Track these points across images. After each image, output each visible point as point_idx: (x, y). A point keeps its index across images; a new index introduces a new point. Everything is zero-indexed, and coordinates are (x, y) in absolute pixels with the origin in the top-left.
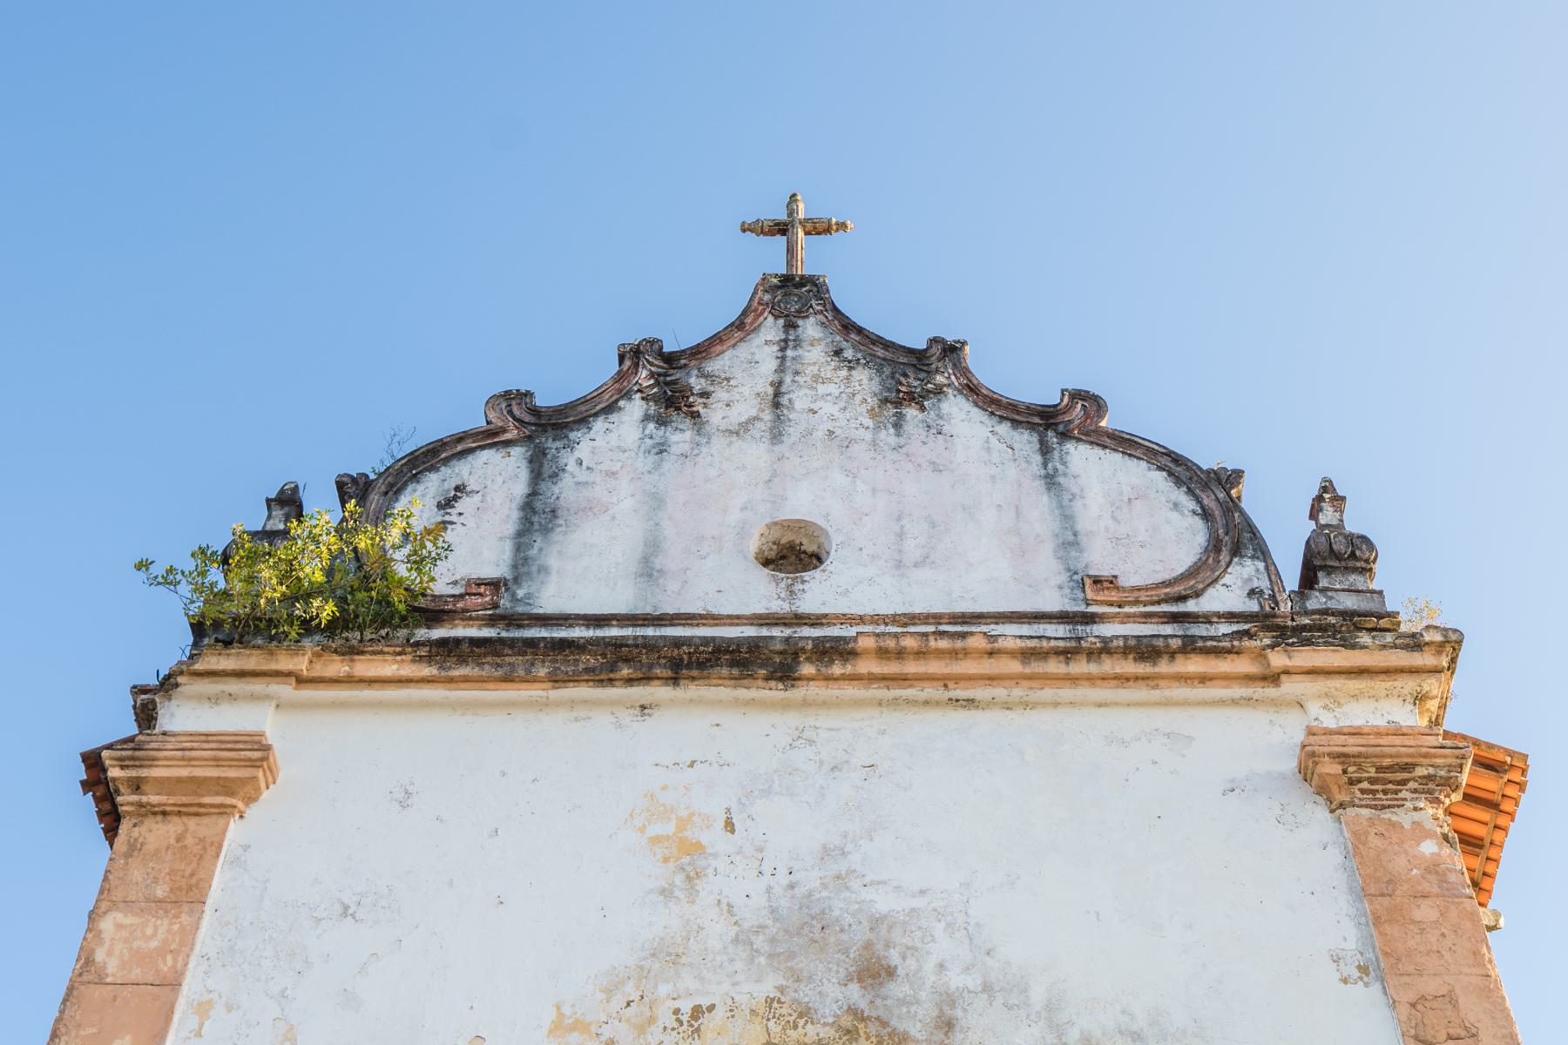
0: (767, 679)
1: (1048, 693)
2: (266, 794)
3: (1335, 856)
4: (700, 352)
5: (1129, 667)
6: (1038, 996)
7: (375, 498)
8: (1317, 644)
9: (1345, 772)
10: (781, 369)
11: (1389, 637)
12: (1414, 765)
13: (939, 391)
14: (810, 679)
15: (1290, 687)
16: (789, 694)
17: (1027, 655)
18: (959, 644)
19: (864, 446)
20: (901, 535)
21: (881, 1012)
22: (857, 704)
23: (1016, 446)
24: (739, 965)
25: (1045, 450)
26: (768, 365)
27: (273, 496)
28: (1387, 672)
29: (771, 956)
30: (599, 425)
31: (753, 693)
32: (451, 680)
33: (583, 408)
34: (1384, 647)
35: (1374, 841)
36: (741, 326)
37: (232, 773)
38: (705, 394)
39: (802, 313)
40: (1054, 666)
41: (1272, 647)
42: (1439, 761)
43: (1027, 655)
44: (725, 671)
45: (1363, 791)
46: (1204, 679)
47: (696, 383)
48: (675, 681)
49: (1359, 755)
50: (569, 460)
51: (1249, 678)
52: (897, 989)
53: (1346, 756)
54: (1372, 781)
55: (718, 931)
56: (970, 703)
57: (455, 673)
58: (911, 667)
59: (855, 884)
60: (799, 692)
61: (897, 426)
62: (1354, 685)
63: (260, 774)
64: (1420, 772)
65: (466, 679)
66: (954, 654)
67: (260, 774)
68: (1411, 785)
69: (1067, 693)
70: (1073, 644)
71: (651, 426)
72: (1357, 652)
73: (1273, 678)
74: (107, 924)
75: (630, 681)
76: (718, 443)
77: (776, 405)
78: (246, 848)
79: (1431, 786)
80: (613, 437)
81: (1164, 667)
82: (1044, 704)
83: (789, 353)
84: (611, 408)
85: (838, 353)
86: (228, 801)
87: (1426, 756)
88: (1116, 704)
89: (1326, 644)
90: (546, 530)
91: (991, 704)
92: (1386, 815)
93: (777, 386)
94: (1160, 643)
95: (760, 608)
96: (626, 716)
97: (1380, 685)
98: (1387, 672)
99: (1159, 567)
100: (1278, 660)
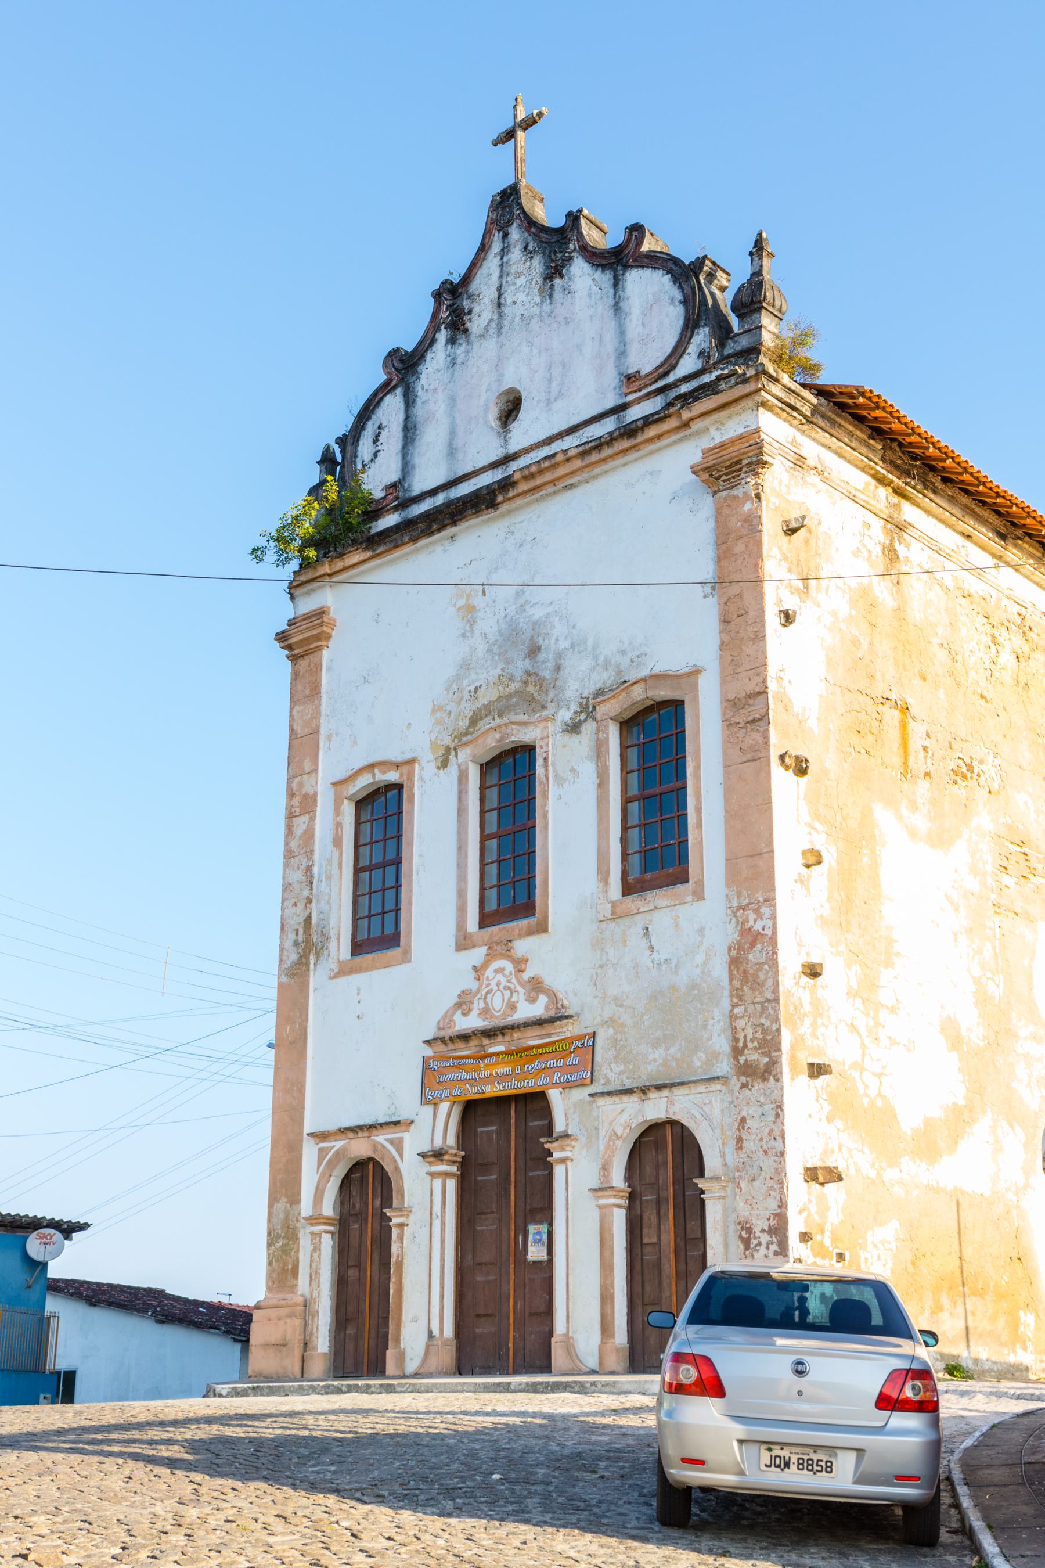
0: (487, 508)
1: (597, 471)
2: (334, 633)
3: (712, 524)
4: (467, 278)
5: (625, 444)
6: (590, 643)
7: (349, 448)
8: (700, 399)
9: (711, 475)
10: (501, 277)
11: (733, 380)
12: (741, 460)
13: (570, 259)
14: (503, 502)
15: (695, 426)
16: (498, 512)
17: (583, 454)
18: (553, 461)
19: (536, 319)
20: (550, 381)
21: (536, 670)
22: (528, 504)
23: (603, 287)
24: (489, 663)
25: (616, 283)
26: (496, 273)
27: (319, 459)
28: (736, 401)
29: (499, 655)
30: (429, 356)
31: (485, 517)
32: (378, 555)
33: (420, 348)
34: (731, 387)
35: (726, 511)
36: (483, 248)
37: (315, 632)
38: (470, 312)
39: (509, 224)
40: (595, 457)
41: (682, 408)
42: (750, 454)
43: (583, 454)
44: (470, 512)
45: (724, 481)
46: (659, 437)
47: (466, 304)
48: (454, 523)
49: (714, 465)
50: (418, 389)
51: (678, 429)
52: (542, 656)
53: (709, 467)
54: (726, 474)
55: (481, 647)
56: (571, 486)
57: (378, 551)
58: (539, 481)
59: (527, 607)
60: (504, 508)
61: (551, 296)
62: (724, 414)
63: (325, 628)
64: (745, 462)
65: (383, 552)
66: (554, 466)
67: (325, 628)
68: (744, 470)
69: (605, 467)
70: (598, 442)
71: (449, 346)
72: (720, 395)
73: (686, 425)
74: (295, 713)
75: (439, 530)
76: (476, 345)
77: (499, 305)
78: (332, 660)
79: (753, 467)
80: (434, 361)
81: (640, 438)
82: (601, 474)
83: (505, 259)
84: (433, 341)
85: (526, 248)
86: (319, 643)
87: (744, 454)
88: (631, 462)
89: (707, 395)
90: (413, 440)
91: (580, 483)
92: (734, 492)
93: (499, 289)
94: (633, 426)
95: (493, 458)
96: (447, 543)
97: (737, 408)
98: (736, 401)
99: (659, 354)
100: (686, 415)
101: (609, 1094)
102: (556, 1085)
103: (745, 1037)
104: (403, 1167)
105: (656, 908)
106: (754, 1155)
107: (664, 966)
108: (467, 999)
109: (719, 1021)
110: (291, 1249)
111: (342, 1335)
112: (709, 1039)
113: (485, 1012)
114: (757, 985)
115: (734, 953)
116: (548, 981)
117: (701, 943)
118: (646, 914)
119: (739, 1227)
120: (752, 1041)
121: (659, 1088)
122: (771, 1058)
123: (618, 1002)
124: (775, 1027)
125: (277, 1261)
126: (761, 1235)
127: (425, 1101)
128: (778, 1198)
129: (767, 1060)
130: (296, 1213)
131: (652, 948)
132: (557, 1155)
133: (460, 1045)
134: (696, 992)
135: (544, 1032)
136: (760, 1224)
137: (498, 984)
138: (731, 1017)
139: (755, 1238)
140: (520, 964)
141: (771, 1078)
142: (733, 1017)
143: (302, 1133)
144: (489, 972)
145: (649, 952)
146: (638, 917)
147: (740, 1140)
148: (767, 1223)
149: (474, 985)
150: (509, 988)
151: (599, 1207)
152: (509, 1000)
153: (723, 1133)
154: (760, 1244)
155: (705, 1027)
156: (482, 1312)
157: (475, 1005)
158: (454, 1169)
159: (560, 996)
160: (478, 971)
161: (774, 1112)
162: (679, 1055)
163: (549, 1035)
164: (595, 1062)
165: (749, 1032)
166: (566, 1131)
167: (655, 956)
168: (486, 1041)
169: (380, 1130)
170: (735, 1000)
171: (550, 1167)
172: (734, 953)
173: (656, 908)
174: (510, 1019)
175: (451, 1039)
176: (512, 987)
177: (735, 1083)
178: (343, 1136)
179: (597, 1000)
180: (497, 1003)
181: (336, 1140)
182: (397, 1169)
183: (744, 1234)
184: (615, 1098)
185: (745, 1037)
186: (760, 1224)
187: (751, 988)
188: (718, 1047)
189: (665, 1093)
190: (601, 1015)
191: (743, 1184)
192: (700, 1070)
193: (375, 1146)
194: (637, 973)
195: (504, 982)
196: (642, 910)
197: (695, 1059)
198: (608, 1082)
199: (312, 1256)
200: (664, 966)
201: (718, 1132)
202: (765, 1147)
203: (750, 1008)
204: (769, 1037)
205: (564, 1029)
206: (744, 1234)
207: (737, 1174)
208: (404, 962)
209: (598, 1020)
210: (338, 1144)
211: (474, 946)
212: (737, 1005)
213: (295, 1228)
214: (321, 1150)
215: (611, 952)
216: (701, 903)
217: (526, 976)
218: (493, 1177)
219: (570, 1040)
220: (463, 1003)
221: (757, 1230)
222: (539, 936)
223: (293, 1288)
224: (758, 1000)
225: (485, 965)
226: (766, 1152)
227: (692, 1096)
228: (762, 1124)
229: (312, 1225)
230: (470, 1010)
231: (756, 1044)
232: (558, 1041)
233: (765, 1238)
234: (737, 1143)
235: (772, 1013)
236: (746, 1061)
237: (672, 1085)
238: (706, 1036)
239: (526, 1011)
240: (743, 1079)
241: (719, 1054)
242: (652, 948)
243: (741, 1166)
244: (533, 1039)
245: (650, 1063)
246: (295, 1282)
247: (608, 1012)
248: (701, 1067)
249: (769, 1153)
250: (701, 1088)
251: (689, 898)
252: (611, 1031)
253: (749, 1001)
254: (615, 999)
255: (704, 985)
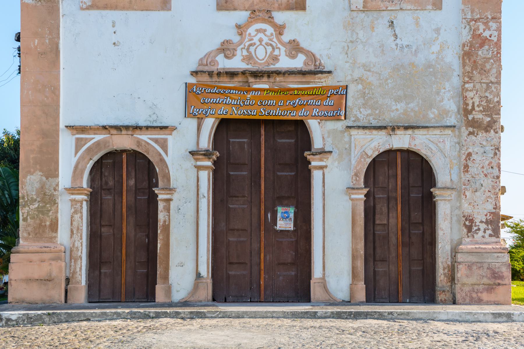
101: (359, 127)
102: (315, 117)
103: (473, 103)
104: (168, 160)
105: (401, 9)
106: (477, 176)
107: (406, 50)
108: (231, 47)
109: (449, 91)
110: (50, 211)
111: (97, 273)
112: (442, 100)
113: (249, 58)
114: (484, 71)
115: (467, 48)
116: (303, 44)
117: (437, 38)
118: (392, 12)
119: (464, 219)
120: (478, 106)
121: (406, 128)
122: (492, 118)
123: (366, 67)
124: (496, 100)
125: (33, 218)
126: (480, 224)
127: (188, 114)
128: (494, 203)
129: (489, 119)
130: (54, 185)
131: (396, 36)
132: (313, 163)
133: (225, 79)
134: (431, 70)
135: (304, 80)
136: (479, 217)
137: (261, 40)
138: (463, 89)
139: (476, 226)
140: (280, 29)
141: (492, 131)
142: (464, 89)
143: (58, 124)
144: (252, 30)
145: (393, 38)
146: (385, 13)
147: (466, 167)
148: (485, 217)
149: (236, 39)
150: (271, 45)
151: (352, 200)
152: (271, 53)
153: (451, 161)
154: (479, 229)
155: (438, 93)
156: (235, 261)
157: (239, 52)
158: (209, 163)
159: (318, 56)
160: (241, 29)
161: (493, 152)
162: (417, 109)
163: (308, 83)
164: (347, 106)
165: (477, 101)
166: (323, 148)
167: (398, 41)
168: (251, 80)
169: (144, 131)
170: (467, 79)
171: (309, 171)
172: (467, 48)
173: (401, 9)
174: (272, 66)
175: (219, 74)
176: (274, 44)
177: (465, 131)
178: (104, 131)
179: (348, 64)
180: (261, 53)
181: (95, 134)
182: (162, 160)
183: (467, 223)
184: (367, 131)
185: (473, 103)
186: (479, 217)
187: (479, 73)
188: (448, 107)
189: (410, 132)
190: (351, 75)
191: (467, 193)
192: (433, 120)
193: (139, 142)
194: (383, 50)
195: (266, 40)
196: (389, 8)
197: (429, 113)
198: (357, 119)
199: (72, 218)
200: (406, 50)
201: (448, 160)
202: (485, 172)
203: (478, 86)
204: (491, 106)
205: (322, 80)
206: (467, 223)
207: (464, 187)
208: (163, 9)
209: (349, 77)
210: (98, 137)
211: (235, 9)
212: (468, 82)
213: (52, 195)
214: (77, 139)
215: (361, 34)
216: (438, 12)
217: (286, 37)
218: (245, 173)
219: (328, 88)
220: (226, 49)
221: (477, 221)
222: (296, 12)
223: (52, 239)
224: (484, 81)
225: (248, 24)
226: (486, 175)
227: (428, 136)
228: (484, 158)
229: (72, 194)
230: (234, 55)
231: (481, 108)
232: (316, 88)
233: (483, 226)
234: (465, 168)
235: (495, 90)
236: (474, 118)
237: (418, 127)
238: (438, 99)
239: (285, 63)
240: (471, 129)
241: (449, 111)
242: (396, 36)
243: (467, 182)
244: (293, 83)
245: (393, 111)
246: (54, 235)
247: (357, 74)
248: (434, 118)
249: (489, 176)
250: (437, 132)
251: (430, 7)
252: (360, 87)
253: (478, 81)
254: (364, 66)
255: (439, 66)
